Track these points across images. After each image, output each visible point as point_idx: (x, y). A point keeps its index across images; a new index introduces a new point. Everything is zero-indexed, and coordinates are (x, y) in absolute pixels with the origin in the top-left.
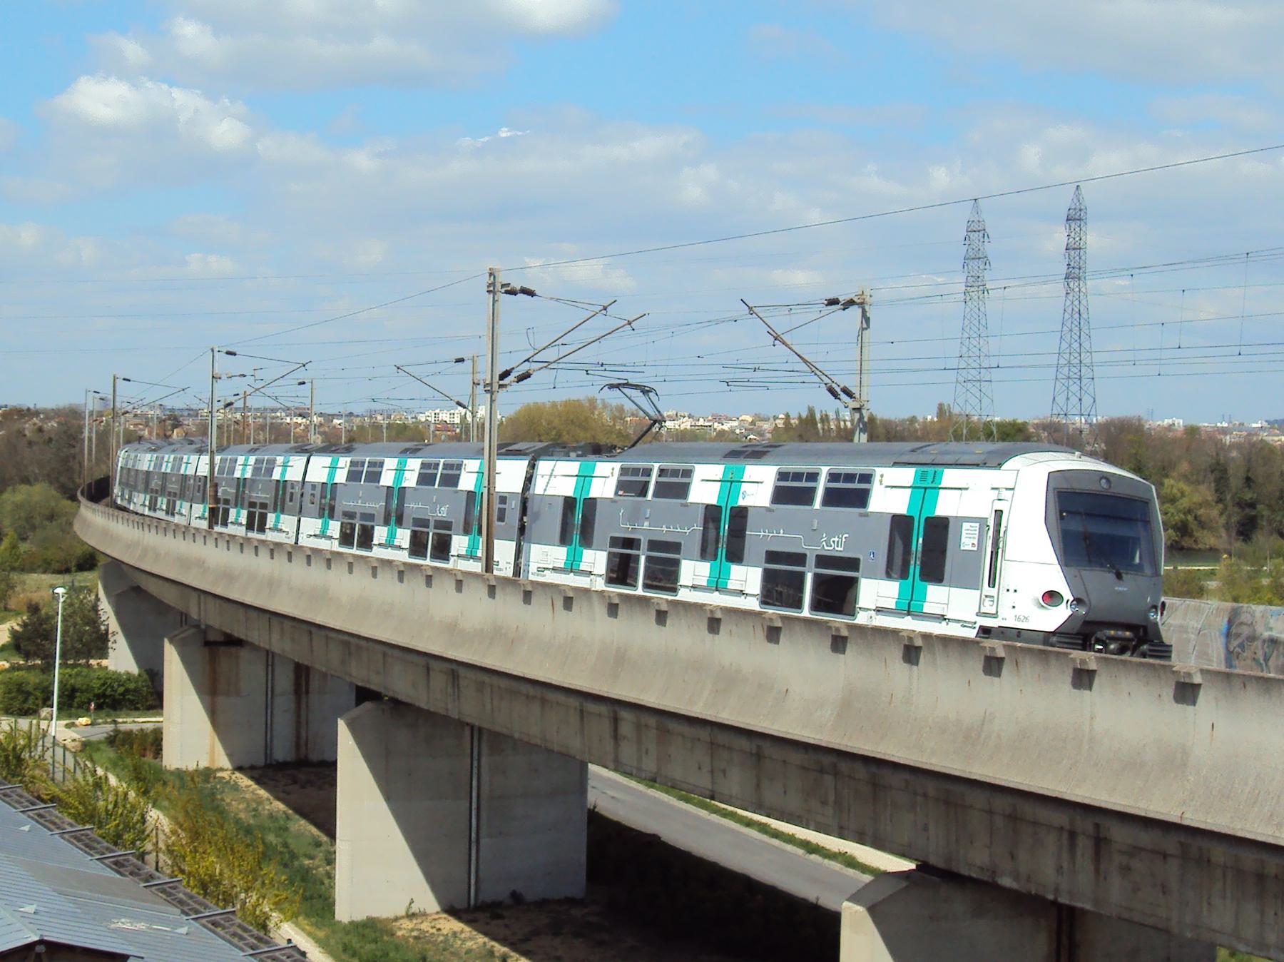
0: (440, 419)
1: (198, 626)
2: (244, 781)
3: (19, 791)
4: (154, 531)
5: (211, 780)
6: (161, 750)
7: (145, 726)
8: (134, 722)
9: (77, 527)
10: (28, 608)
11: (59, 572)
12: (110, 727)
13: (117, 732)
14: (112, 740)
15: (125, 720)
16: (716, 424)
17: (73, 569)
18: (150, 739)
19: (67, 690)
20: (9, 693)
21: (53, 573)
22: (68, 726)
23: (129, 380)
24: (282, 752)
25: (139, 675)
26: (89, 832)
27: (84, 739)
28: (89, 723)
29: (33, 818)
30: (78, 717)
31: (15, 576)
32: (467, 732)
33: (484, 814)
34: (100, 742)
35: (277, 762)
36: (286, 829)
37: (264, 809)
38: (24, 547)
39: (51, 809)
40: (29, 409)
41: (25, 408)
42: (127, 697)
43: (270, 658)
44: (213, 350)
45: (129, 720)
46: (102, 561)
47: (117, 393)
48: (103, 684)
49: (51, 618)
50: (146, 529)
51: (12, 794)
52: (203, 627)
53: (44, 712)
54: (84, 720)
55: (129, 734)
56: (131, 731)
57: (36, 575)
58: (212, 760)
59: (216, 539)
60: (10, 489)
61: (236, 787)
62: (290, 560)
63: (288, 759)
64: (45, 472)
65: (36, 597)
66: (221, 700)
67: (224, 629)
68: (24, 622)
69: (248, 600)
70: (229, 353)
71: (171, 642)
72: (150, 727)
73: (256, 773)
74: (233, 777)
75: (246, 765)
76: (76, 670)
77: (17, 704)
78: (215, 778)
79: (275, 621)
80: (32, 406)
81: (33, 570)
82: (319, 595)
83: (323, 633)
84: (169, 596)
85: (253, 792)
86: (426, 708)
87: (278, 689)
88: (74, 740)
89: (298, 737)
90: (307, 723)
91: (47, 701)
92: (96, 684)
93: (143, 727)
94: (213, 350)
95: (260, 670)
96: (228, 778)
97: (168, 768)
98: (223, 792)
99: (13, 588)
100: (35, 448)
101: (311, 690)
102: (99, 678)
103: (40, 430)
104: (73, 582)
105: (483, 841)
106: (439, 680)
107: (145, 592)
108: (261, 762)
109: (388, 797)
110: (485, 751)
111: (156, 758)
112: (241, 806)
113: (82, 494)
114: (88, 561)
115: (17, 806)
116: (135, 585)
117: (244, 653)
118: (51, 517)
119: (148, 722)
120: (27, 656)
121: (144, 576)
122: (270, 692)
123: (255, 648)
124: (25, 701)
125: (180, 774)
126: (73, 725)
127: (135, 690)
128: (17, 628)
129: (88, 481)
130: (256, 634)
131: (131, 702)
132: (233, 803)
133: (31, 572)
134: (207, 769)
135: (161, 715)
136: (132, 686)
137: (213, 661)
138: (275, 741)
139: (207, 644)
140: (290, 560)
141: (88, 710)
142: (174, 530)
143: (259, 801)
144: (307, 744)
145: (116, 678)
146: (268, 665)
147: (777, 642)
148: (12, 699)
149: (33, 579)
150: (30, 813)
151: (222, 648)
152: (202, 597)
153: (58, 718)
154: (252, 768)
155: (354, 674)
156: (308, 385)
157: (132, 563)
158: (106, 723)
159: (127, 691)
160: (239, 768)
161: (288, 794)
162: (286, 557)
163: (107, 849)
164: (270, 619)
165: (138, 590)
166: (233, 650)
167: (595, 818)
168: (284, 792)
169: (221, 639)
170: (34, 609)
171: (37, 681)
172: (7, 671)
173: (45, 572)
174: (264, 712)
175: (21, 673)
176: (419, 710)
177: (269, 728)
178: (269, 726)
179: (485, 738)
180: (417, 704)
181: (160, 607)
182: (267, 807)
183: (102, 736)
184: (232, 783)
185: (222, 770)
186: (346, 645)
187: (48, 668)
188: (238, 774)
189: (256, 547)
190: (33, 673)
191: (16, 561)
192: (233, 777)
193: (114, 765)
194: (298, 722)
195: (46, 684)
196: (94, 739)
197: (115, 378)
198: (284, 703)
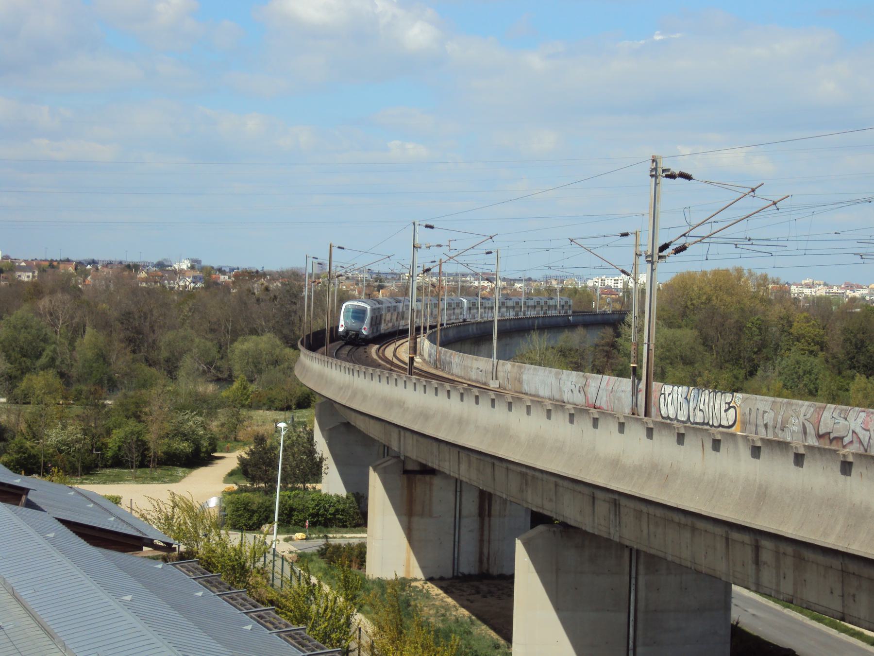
0: (606, 284)
1: (398, 457)
2: (435, 590)
3: (244, 595)
4: (362, 375)
5: (407, 588)
6: (365, 561)
7: (351, 541)
8: (343, 537)
9: (297, 372)
10: (256, 439)
11: (282, 409)
12: (321, 542)
13: (328, 546)
14: (322, 553)
15: (335, 535)
16: (848, 291)
17: (293, 407)
18: (356, 553)
19: (286, 509)
20: (237, 511)
21: (276, 409)
22: (286, 540)
23: (343, 248)
24: (467, 566)
25: (347, 497)
26: (302, 632)
27: (299, 551)
28: (304, 537)
29: (254, 619)
30: (295, 532)
31: (244, 412)
32: (626, 554)
33: (640, 626)
34: (312, 554)
35: (464, 575)
36: (469, 633)
37: (451, 614)
38: (252, 387)
39: (270, 611)
40: (257, 272)
41: (254, 270)
42: (337, 516)
43: (458, 485)
44: (414, 224)
45: (338, 535)
46: (318, 400)
47: (333, 259)
48: (317, 505)
49: (274, 448)
50: (356, 374)
51: (238, 598)
52: (402, 458)
53: (265, 528)
54: (299, 535)
55: (338, 547)
56: (340, 545)
57: (261, 411)
58: (408, 571)
59: (415, 384)
60: (240, 338)
61: (427, 596)
62: (477, 403)
64: (270, 325)
65: (261, 430)
66: (415, 519)
67: (420, 460)
68: (251, 450)
69: (441, 436)
70: (428, 226)
71: (375, 470)
72: (355, 542)
73: (444, 584)
74: (426, 586)
75: (436, 576)
76: (294, 492)
77: (243, 521)
78: (410, 586)
79: (463, 455)
80: (260, 269)
81: (258, 408)
82: (502, 433)
83: (504, 465)
84: (374, 431)
85: (442, 600)
86: (591, 531)
87: (465, 512)
88: (291, 552)
89: (481, 553)
90: (489, 542)
91: (268, 519)
92: (311, 504)
94: (414, 224)
95: (449, 496)
96: (421, 588)
97: (370, 577)
98: (415, 600)
99: (240, 421)
100: (262, 304)
101: (493, 512)
102: (313, 500)
103: (267, 289)
104: (293, 418)
106: (603, 508)
107: (354, 427)
108: (449, 574)
109: (558, 609)
110: (641, 568)
111: (360, 569)
112: (431, 612)
113: (302, 343)
114: (305, 401)
116: (345, 421)
117: (437, 481)
118: (276, 362)
119: (354, 538)
120: (253, 479)
121: (353, 414)
122: (458, 518)
123: (447, 477)
124: (252, 516)
125: (381, 584)
126: (291, 539)
127: (343, 511)
128: (245, 456)
129: (307, 333)
130: (447, 464)
131: (340, 520)
132: (425, 608)
133: (259, 409)
134: (404, 579)
135: (365, 532)
136: (341, 507)
137: (410, 487)
138: (461, 558)
139: (406, 472)
140: (477, 403)
141: (304, 526)
142: (379, 376)
143: (447, 608)
144: (488, 559)
145: (327, 498)
146: (456, 491)
147: (683, 444)
148: (240, 516)
150: (252, 614)
151: (419, 476)
152: (402, 433)
154: (442, 579)
155: (530, 500)
156: (494, 255)
157: (343, 403)
158: (318, 538)
159: (337, 510)
160: (430, 579)
162: (474, 400)
163: (318, 647)
164: (459, 452)
165: (348, 425)
166: (428, 478)
167: (737, 633)
168: (468, 600)
169: (417, 468)
170: (260, 440)
171: (261, 501)
172: (236, 492)
173: (269, 409)
174: (452, 532)
175: (248, 494)
176: (585, 533)
177: (456, 544)
178: (456, 543)
179: (642, 559)
180: (583, 529)
181: (367, 440)
182: (454, 613)
183: (314, 550)
184: (425, 591)
185: (415, 580)
186: (523, 475)
187: (272, 490)
188: (429, 584)
189: (449, 392)
190: (258, 494)
191: (247, 399)
192: (426, 586)
193: (327, 574)
194: (481, 541)
195: (268, 503)
196: (306, 551)
198: (470, 524)
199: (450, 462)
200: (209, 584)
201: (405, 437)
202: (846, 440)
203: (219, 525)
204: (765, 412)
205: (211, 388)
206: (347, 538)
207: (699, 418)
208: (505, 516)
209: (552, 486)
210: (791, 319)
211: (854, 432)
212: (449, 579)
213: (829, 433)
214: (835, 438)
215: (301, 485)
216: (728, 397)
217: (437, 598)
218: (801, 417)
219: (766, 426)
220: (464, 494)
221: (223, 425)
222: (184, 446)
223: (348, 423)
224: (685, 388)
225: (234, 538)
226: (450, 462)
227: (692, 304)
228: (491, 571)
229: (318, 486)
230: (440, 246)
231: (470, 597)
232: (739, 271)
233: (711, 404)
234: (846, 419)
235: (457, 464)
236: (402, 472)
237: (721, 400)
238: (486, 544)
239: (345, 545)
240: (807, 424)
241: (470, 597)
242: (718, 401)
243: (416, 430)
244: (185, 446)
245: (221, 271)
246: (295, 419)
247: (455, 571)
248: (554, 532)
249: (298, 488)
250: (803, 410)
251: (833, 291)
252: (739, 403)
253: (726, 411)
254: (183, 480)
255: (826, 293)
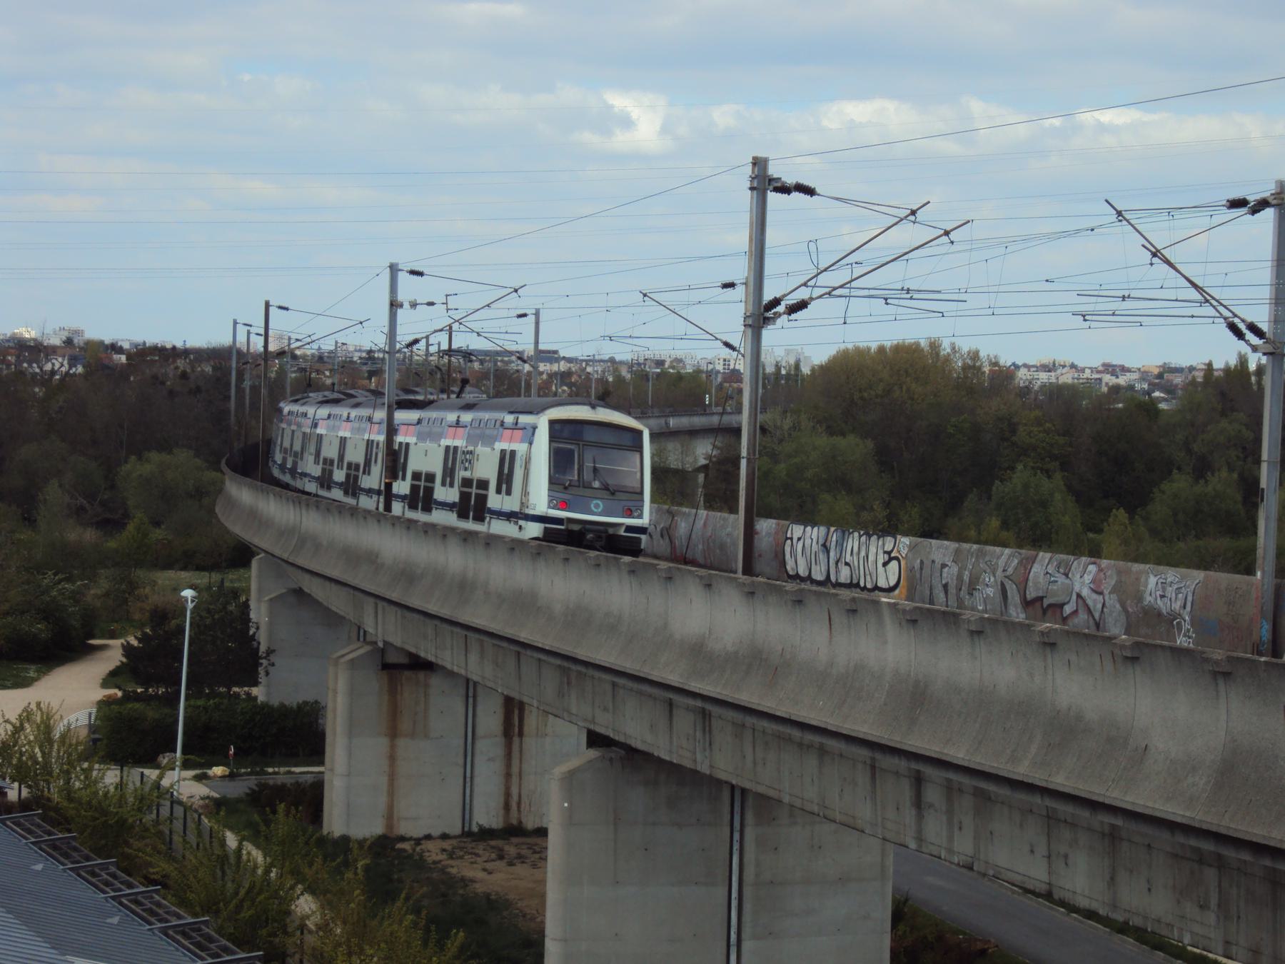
0: (732, 367)
1: (376, 643)
7: (302, 779)
13: (262, 786)
15: (276, 769)
21: (199, 568)
22: (198, 778)
23: (287, 309)
24: (487, 814)
28: (227, 773)
31: (141, 574)
32: (726, 795)
33: (747, 907)
34: (239, 800)
35: (480, 827)
38: (158, 534)
40: (174, 348)
41: (169, 346)
43: (470, 689)
45: (282, 770)
47: (271, 325)
53: (164, 759)
54: (218, 771)
56: (284, 785)
63: (495, 826)
66: (402, 742)
68: (145, 634)
70: (413, 272)
72: (310, 779)
74: (418, 849)
78: (393, 849)
80: (179, 345)
81: (168, 566)
85: (443, 871)
86: (667, 758)
87: (480, 731)
89: (508, 795)
93: (300, 780)
96: (411, 851)
101: (526, 729)
105: (747, 945)
107: (309, 595)
108: (457, 830)
113: (228, 464)
115: (107, 889)
117: (435, 681)
120: (146, 683)
121: (307, 577)
123: (451, 674)
128: (135, 643)
130: (447, 654)
135: (322, 763)
137: (393, 691)
138: (475, 802)
139: (386, 667)
141: (227, 756)
144: (519, 804)
146: (467, 697)
149: (165, 578)
151: (407, 673)
153: (186, 765)
154: (444, 837)
155: (574, 711)
161: (490, 873)
164: (466, 636)
165: (299, 593)
166: (421, 675)
168: (485, 870)
169: (403, 660)
173: (184, 568)
174: (461, 761)
175: (137, 705)
176: (660, 761)
179: (750, 801)
180: (656, 754)
182: (461, 892)
185: (403, 839)
193: (255, 834)
194: (508, 775)
197: (267, 305)
199: (452, 649)
200: (57, 851)
201: (384, 609)
202: (1068, 609)
203: (86, 756)
204: (944, 566)
205: (90, 535)
206: (296, 774)
207: (844, 574)
208: (546, 735)
209: (608, 688)
210: (1015, 420)
211: (1079, 596)
212: (455, 837)
213: (1041, 599)
214: (1050, 606)
215: (222, 690)
216: (889, 543)
217: (435, 868)
218: (999, 573)
219: (945, 586)
220: (479, 699)
221: (107, 595)
222: (38, 629)
223: (300, 588)
224: (823, 529)
225: (111, 777)
226: (452, 649)
227: (862, 398)
228: (524, 820)
229: (255, 691)
230: (431, 304)
231: (489, 866)
232: (935, 345)
233: (863, 554)
234: (1066, 575)
235: (464, 653)
236: (380, 667)
237: (877, 548)
238: (515, 780)
239: (291, 784)
240: (1009, 585)
241: (489, 866)
242: (873, 549)
243: (394, 599)
244: (40, 629)
245: (115, 348)
246: (227, 584)
247: (467, 825)
248: (611, 760)
249: (220, 695)
250: (1001, 562)
251: (1085, 376)
252: (904, 552)
253: (885, 564)
254: (36, 683)
255: (1073, 378)
